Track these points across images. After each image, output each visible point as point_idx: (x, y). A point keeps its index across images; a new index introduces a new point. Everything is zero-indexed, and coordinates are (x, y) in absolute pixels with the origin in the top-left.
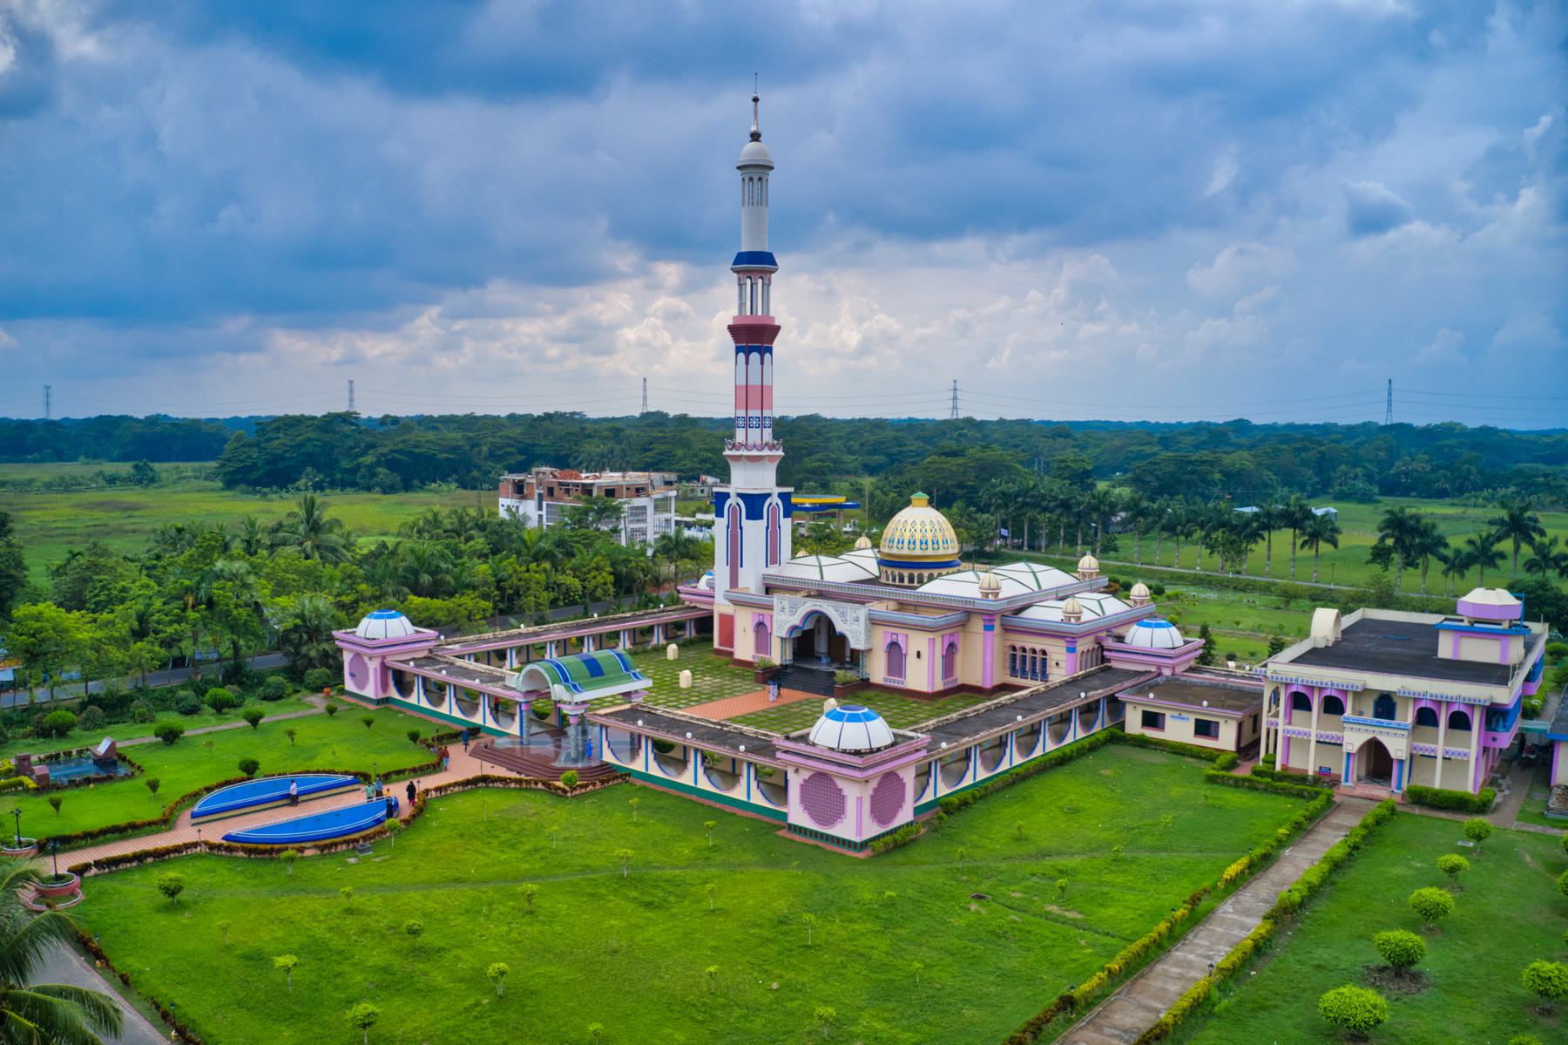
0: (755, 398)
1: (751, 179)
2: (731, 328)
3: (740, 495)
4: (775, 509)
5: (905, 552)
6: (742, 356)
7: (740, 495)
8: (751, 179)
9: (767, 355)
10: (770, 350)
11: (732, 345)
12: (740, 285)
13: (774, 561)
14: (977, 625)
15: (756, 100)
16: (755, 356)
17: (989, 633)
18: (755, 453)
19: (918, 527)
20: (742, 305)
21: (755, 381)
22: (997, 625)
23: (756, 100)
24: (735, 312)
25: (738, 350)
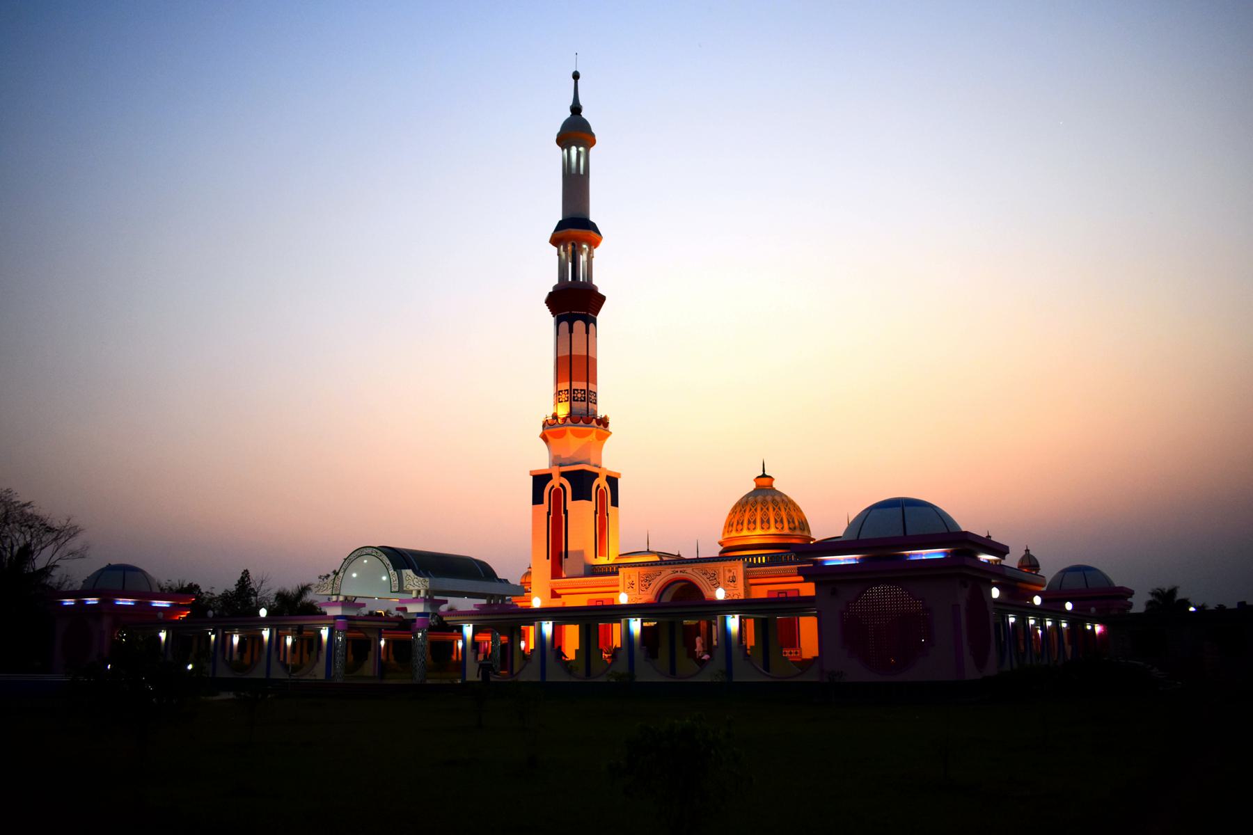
3: (563, 474)
4: (602, 494)
6: (564, 325)
7: (563, 474)
9: (592, 325)
16: (579, 325)
21: (579, 350)
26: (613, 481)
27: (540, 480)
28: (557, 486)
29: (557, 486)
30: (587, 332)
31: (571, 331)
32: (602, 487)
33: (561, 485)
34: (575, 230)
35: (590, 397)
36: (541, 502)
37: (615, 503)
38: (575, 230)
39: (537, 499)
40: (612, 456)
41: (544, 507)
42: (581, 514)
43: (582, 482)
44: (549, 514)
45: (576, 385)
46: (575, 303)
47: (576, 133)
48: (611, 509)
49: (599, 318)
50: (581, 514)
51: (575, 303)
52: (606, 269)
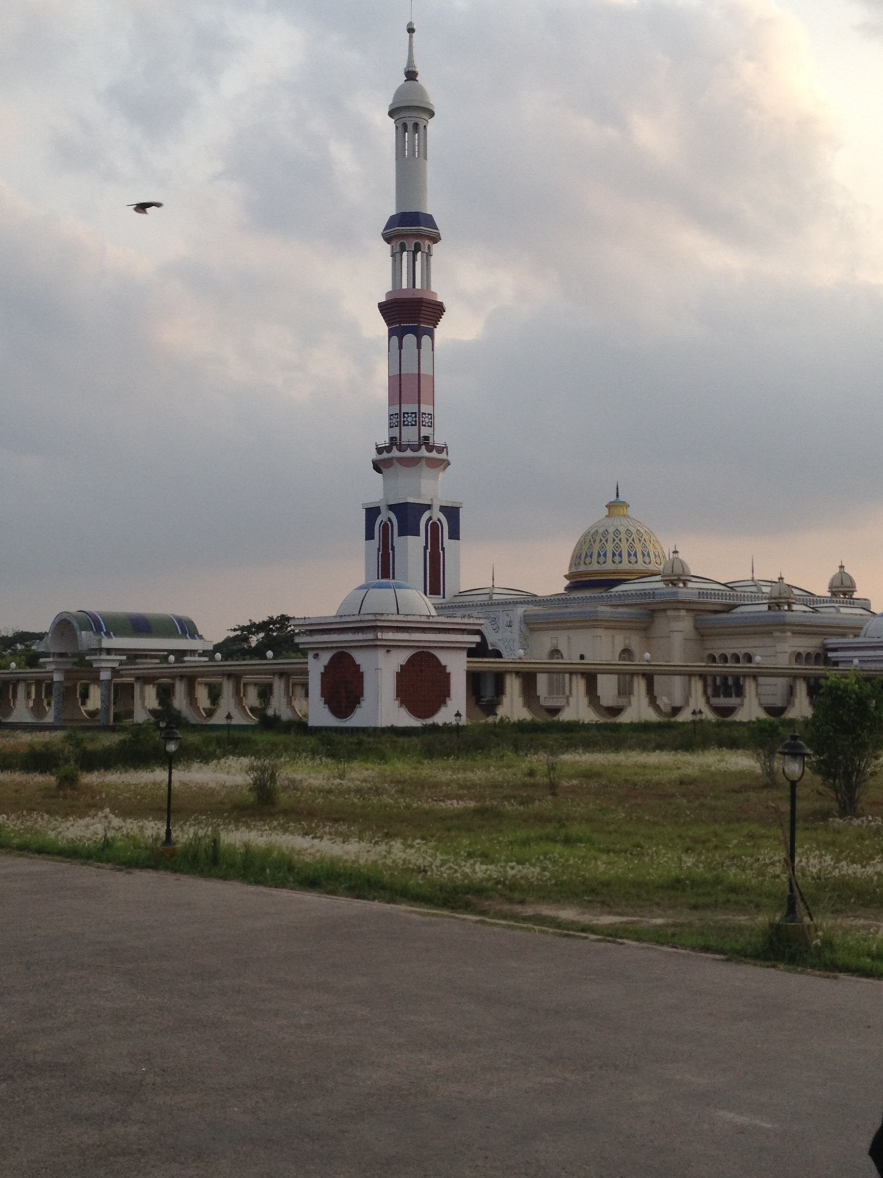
1: (405, 126)
2: (383, 307)
3: (391, 507)
5: (595, 567)
6: (395, 339)
8: (405, 126)
9: (425, 339)
10: (431, 335)
11: (382, 328)
18: (409, 453)
21: (409, 368)
23: (411, 30)
24: (389, 288)
25: (391, 333)
26: (452, 513)
27: (372, 513)
28: (385, 520)
29: (385, 520)
30: (419, 347)
31: (401, 347)
32: (435, 519)
33: (390, 520)
36: (373, 538)
37: (455, 534)
39: (369, 536)
41: (375, 543)
42: (412, 550)
44: (379, 549)
45: (406, 408)
47: (410, 115)
48: (447, 542)
49: (438, 332)
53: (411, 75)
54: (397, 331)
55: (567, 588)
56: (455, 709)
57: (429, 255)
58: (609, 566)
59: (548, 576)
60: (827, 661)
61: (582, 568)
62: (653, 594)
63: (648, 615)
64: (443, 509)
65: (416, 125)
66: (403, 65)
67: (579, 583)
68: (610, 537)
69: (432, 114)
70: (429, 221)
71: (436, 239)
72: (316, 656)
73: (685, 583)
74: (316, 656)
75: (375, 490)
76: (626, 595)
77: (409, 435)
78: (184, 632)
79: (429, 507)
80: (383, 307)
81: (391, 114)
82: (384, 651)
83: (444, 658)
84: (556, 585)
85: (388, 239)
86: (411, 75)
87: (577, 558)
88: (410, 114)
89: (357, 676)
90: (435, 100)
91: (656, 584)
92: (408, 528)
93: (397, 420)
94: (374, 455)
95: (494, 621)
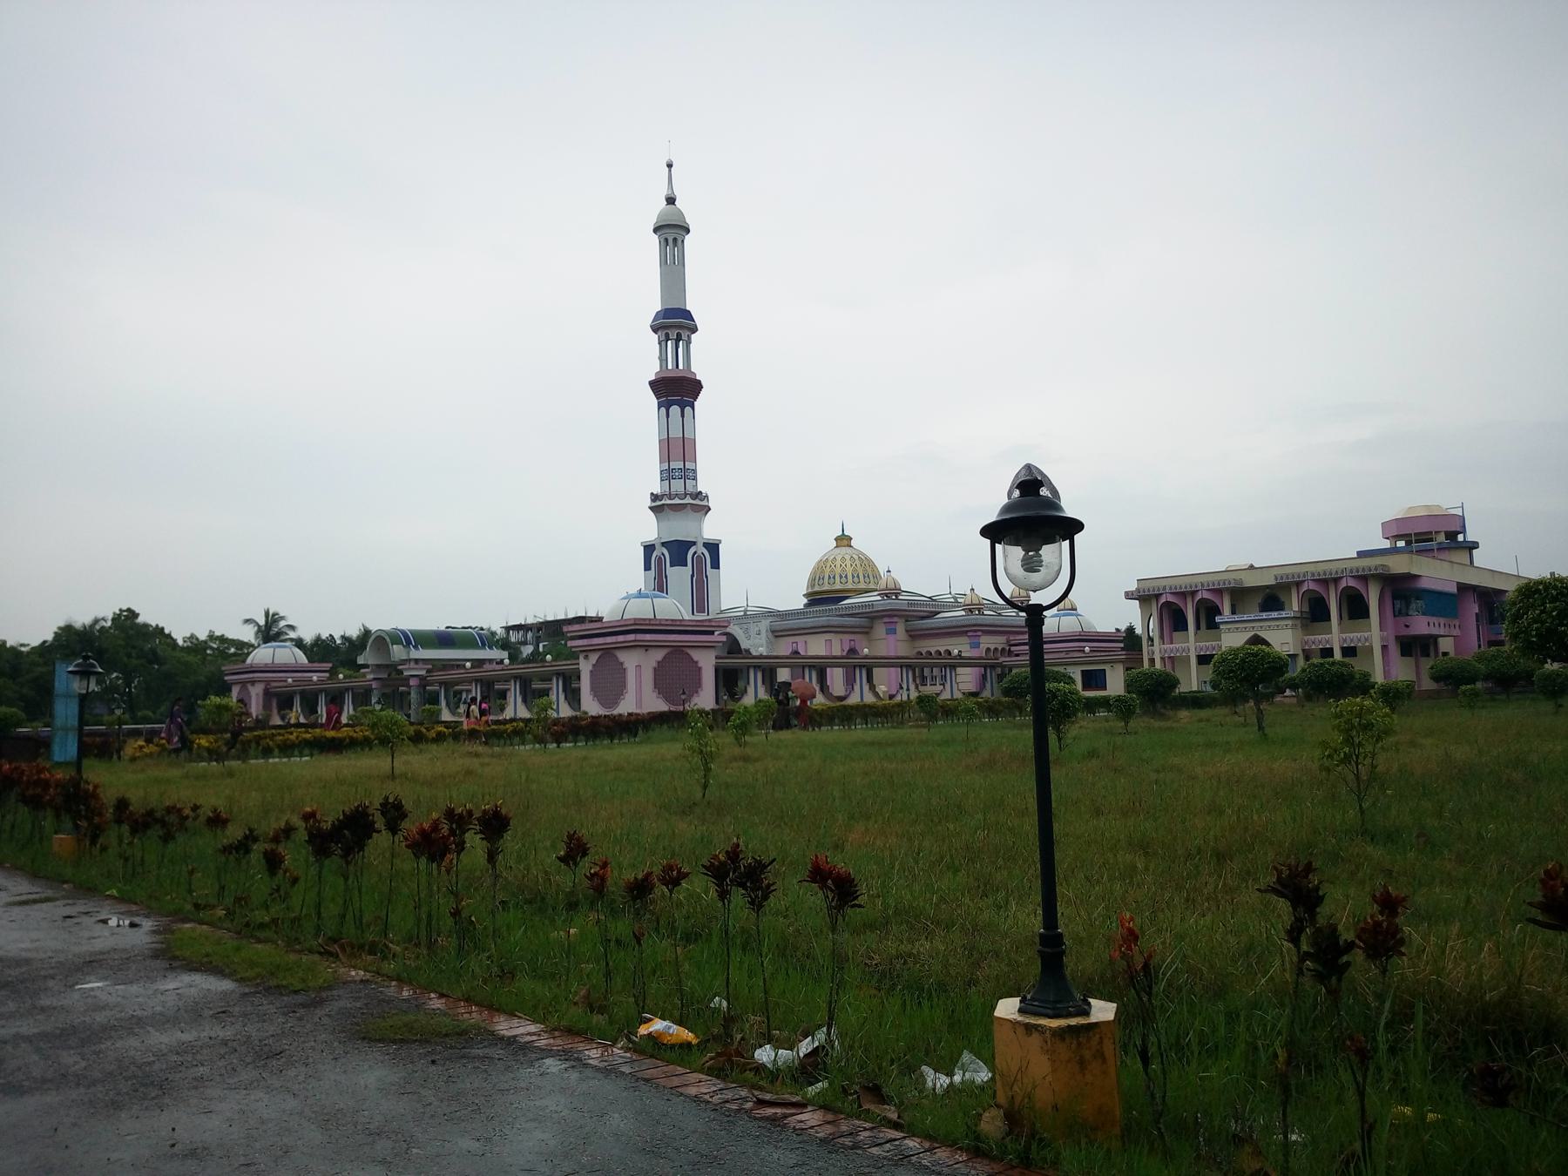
0: (677, 450)
2: (652, 384)
3: (663, 544)
4: (699, 560)
5: (826, 587)
9: (688, 409)
12: (662, 343)
13: (701, 610)
14: (880, 630)
15: (670, 166)
16: (675, 410)
17: (891, 637)
19: (838, 563)
20: (663, 359)
21: (676, 433)
22: (900, 628)
23: (670, 166)
26: (713, 548)
27: (649, 549)
34: (675, 324)
35: (689, 474)
37: (716, 565)
38: (675, 324)
39: (647, 567)
40: (710, 528)
41: (652, 573)
43: (679, 551)
46: (677, 390)
47: (672, 231)
50: (679, 577)
51: (677, 390)
52: (702, 358)
53: (671, 201)
54: (665, 404)
55: (806, 606)
56: (706, 699)
57: (689, 342)
58: (838, 586)
59: (789, 594)
60: (1010, 653)
61: (817, 589)
62: (871, 604)
63: (870, 619)
64: (706, 545)
65: (675, 240)
66: (664, 192)
67: (817, 599)
68: (838, 563)
69: (688, 231)
70: (687, 315)
71: (694, 330)
72: (586, 657)
73: (897, 595)
74: (586, 657)
75: (650, 529)
76: (852, 606)
77: (677, 486)
78: (484, 645)
79: (694, 543)
80: (652, 384)
81: (656, 230)
82: (641, 652)
83: (696, 655)
84: (800, 603)
85: (655, 329)
86: (671, 201)
87: (812, 581)
88: (672, 231)
89: (623, 671)
90: (690, 221)
91: (874, 597)
92: (679, 560)
93: (667, 475)
94: (649, 503)
95: (746, 631)
